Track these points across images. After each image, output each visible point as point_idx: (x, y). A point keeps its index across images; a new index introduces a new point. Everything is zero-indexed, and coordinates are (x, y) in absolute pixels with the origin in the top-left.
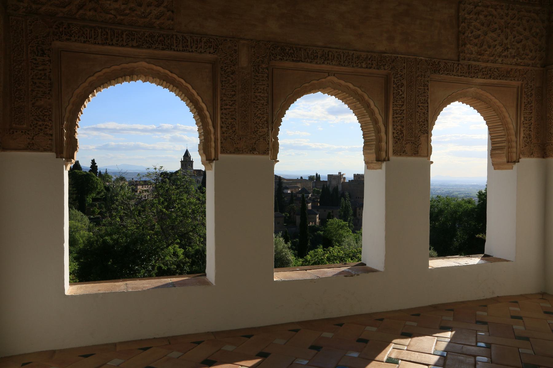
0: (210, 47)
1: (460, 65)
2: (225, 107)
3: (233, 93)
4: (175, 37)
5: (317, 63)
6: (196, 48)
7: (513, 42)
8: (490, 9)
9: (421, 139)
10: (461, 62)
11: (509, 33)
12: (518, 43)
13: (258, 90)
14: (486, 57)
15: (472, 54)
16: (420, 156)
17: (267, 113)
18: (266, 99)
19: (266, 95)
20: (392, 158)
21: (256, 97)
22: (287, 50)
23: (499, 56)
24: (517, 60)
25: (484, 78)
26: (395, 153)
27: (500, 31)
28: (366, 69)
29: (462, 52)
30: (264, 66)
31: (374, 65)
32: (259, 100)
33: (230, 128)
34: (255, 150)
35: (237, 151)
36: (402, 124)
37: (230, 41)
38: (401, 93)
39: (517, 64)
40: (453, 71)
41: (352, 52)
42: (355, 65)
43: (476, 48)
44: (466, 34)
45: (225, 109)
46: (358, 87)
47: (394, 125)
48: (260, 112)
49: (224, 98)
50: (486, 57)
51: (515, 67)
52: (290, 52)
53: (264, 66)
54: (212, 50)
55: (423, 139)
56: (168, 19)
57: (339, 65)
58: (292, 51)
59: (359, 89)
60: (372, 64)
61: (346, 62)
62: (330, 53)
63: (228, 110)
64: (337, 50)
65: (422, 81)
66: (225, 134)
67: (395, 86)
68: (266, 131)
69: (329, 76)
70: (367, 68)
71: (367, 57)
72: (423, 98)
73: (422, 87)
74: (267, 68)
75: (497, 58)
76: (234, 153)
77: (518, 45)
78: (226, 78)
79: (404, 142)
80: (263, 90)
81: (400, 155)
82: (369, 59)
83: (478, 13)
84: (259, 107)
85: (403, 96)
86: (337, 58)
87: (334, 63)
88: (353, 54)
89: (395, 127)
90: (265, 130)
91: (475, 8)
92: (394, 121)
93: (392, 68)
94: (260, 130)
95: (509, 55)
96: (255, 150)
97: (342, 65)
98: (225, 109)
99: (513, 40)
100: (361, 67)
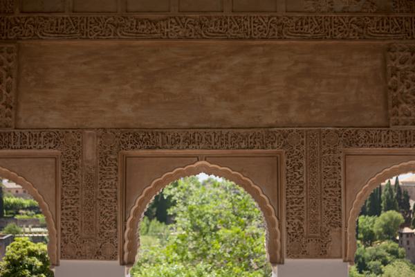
0: (50, 141)
1: (391, 133)
2: (67, 207)
3: (77, 190)
4: (12, 134)
5: (178, 148)
6: (35, 144)
9: (331, 234)
10: (392, 128)
15: (410, 115)
16: (329, 257)
17: (115, 211)
18: (114, 195)
19: (115, 190)
20: (287, 261)
21: (103, 193)
22: (141, 137)
26: (291, 255)
28: (247, 150)
29: (393, 115)
30: (112, 157)
31: (258, 144)
32: (106, 196)
33: (71, 230)
35: (81, 256)
36: (301, 216)
37: (73, 132)
38: (298, 176)
40: (380, 141)
41: (227, 131)
42: (230, 146)
44: (400, 90)
45: (66, 209)
47: (287, 218)
49: (65, 197)
53: (112, 157)
54: (52, 145)
55: (333, 234)
56: (6, 117)
57: (209, 148)
60: (255, 143)
61: (219, 144)
62: (196, 135)
63: (69, 210)
64: (205, 130)
65: (331, 157)
66: (66, 237)
67: (289, 167)
69: (198, 160)
70: (247, 148)
71: (247, 136)
72: (334, 180)
73: (332, 167)
74: (116, 160)
76: (75, 258)
78: (68, 174)
79: (304, 240)
80: (112, 184)
81: (298, 257)
82: (251, 138)
85: (301, 179)
86: (206, 140)
87: (201, 146)
88: (228, 133)
89: (290, 220)
90: (113, 231)
91: (412, 55)
92: (287, 214)
93: (284, 146)
98: (66, 209)
100: (240, 148)
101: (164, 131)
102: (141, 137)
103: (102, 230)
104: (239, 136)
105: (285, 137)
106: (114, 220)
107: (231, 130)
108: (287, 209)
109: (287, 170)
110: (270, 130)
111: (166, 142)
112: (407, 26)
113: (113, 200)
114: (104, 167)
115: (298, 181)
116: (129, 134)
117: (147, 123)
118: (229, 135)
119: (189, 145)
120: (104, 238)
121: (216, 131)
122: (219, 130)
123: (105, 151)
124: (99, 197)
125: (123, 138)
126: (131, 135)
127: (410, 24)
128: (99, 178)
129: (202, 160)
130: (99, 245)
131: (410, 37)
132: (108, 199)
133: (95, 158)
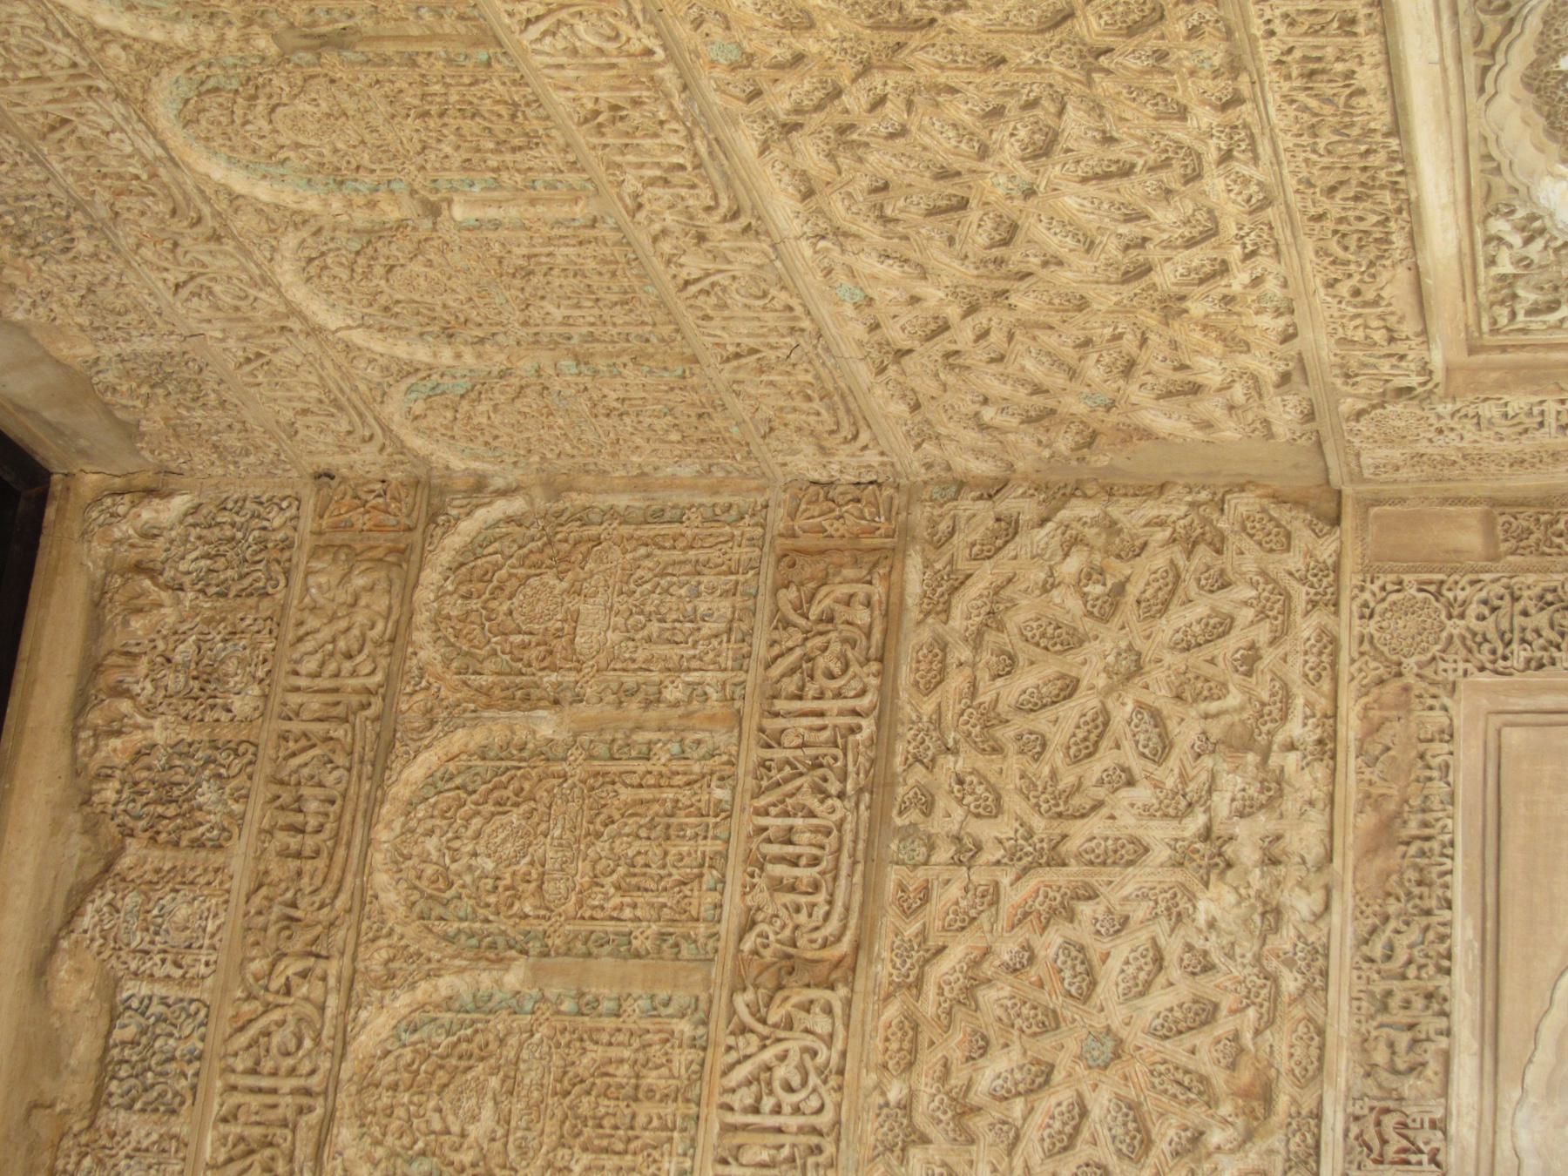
7: (1158, 786)
8: (929, 1005)
11: (1096, 824)
12: (1162, 750)
14: (1283, 1046)
23: (1274, 914)
24: (1291, 747)
25: (1446, 1058)
27: (1085, 909)
39: (1326, 748)
43: (1216, 1137)
50: (1283, 1046)
51: (1350, 763)
75: (1285, 940)
77: (1186, 733)
83: (963, 1110)
91: (925, 1140)
95: (1263, 823)
99: (1143, 794)
112: (765, 1156)
127: (758, 1138)
131: (829, 1149)
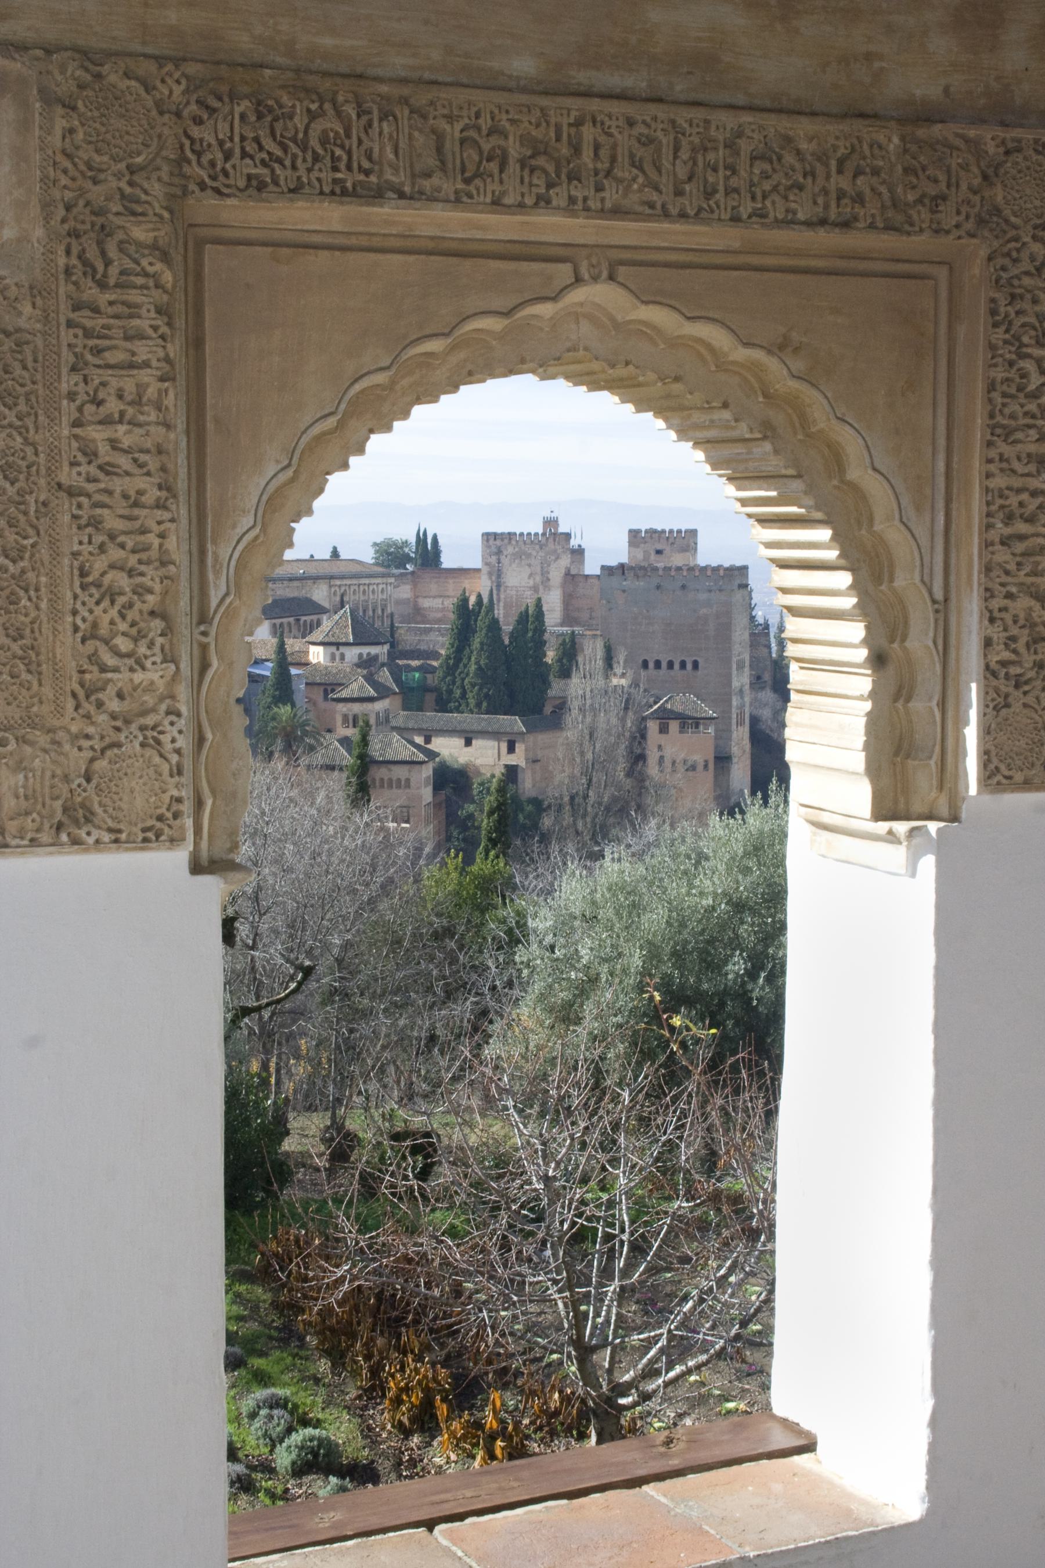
13: (100, 403)
19: (158, 432)
22: (299, 121)
30: (140, 233)
34: (89, 817)
41: (729, 120)
46: (770, 352)
47: (989, 593)
48: (115, 554)
52: (317, 127)
53: (140, 233)
58: (330, 123)
59: (772, 364)
62: (588, 133)
67: (999, 335)
68: (161, 685)
69: (578, 280)
70: (823, 222)
71: (822, 158)
80: (138, 402)
84: (112, 522)
87: (611, 195)
88: (740, 134)
90: (155, 675)
92: (988, 569)
94: (121, 679)
96: (89, 817)
97: (666, 215)
101: (421, 98)
102: (299, 121)
103: (93, 675)
104: (789, 159)
105: (985, 177)
106: (152, 613)
107: (746, 118)
108: (988, 544)
109: (992, 347)
110: (921, 133)
111: (431, 161)
113: (149, 499)
114: (91, 292)
115: (1032, 407)
116: (233, 97)
117: (328, 42)
118: (745, 147)
119: (550, 185)
120: (102, 718)
121: (683, 116)
122: (698, 114)
123: (97, 193)
124: (66, 476)
125: (198, 121)
126: (245, 105)
128: (67, 358)
129: (595, 279)
130: (77, 759)
132: (118, 485)
133: (39, 232)
